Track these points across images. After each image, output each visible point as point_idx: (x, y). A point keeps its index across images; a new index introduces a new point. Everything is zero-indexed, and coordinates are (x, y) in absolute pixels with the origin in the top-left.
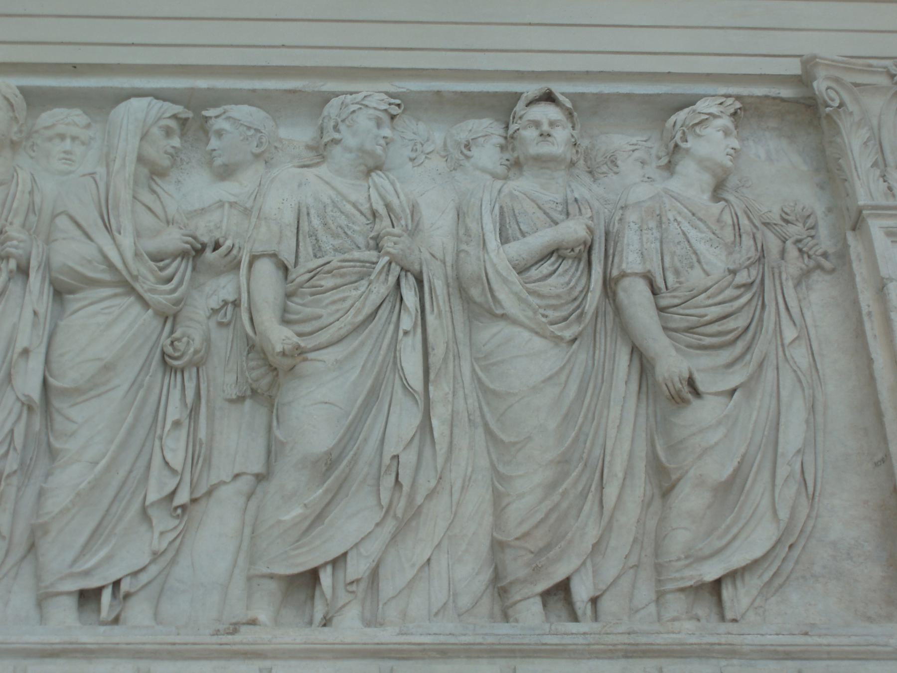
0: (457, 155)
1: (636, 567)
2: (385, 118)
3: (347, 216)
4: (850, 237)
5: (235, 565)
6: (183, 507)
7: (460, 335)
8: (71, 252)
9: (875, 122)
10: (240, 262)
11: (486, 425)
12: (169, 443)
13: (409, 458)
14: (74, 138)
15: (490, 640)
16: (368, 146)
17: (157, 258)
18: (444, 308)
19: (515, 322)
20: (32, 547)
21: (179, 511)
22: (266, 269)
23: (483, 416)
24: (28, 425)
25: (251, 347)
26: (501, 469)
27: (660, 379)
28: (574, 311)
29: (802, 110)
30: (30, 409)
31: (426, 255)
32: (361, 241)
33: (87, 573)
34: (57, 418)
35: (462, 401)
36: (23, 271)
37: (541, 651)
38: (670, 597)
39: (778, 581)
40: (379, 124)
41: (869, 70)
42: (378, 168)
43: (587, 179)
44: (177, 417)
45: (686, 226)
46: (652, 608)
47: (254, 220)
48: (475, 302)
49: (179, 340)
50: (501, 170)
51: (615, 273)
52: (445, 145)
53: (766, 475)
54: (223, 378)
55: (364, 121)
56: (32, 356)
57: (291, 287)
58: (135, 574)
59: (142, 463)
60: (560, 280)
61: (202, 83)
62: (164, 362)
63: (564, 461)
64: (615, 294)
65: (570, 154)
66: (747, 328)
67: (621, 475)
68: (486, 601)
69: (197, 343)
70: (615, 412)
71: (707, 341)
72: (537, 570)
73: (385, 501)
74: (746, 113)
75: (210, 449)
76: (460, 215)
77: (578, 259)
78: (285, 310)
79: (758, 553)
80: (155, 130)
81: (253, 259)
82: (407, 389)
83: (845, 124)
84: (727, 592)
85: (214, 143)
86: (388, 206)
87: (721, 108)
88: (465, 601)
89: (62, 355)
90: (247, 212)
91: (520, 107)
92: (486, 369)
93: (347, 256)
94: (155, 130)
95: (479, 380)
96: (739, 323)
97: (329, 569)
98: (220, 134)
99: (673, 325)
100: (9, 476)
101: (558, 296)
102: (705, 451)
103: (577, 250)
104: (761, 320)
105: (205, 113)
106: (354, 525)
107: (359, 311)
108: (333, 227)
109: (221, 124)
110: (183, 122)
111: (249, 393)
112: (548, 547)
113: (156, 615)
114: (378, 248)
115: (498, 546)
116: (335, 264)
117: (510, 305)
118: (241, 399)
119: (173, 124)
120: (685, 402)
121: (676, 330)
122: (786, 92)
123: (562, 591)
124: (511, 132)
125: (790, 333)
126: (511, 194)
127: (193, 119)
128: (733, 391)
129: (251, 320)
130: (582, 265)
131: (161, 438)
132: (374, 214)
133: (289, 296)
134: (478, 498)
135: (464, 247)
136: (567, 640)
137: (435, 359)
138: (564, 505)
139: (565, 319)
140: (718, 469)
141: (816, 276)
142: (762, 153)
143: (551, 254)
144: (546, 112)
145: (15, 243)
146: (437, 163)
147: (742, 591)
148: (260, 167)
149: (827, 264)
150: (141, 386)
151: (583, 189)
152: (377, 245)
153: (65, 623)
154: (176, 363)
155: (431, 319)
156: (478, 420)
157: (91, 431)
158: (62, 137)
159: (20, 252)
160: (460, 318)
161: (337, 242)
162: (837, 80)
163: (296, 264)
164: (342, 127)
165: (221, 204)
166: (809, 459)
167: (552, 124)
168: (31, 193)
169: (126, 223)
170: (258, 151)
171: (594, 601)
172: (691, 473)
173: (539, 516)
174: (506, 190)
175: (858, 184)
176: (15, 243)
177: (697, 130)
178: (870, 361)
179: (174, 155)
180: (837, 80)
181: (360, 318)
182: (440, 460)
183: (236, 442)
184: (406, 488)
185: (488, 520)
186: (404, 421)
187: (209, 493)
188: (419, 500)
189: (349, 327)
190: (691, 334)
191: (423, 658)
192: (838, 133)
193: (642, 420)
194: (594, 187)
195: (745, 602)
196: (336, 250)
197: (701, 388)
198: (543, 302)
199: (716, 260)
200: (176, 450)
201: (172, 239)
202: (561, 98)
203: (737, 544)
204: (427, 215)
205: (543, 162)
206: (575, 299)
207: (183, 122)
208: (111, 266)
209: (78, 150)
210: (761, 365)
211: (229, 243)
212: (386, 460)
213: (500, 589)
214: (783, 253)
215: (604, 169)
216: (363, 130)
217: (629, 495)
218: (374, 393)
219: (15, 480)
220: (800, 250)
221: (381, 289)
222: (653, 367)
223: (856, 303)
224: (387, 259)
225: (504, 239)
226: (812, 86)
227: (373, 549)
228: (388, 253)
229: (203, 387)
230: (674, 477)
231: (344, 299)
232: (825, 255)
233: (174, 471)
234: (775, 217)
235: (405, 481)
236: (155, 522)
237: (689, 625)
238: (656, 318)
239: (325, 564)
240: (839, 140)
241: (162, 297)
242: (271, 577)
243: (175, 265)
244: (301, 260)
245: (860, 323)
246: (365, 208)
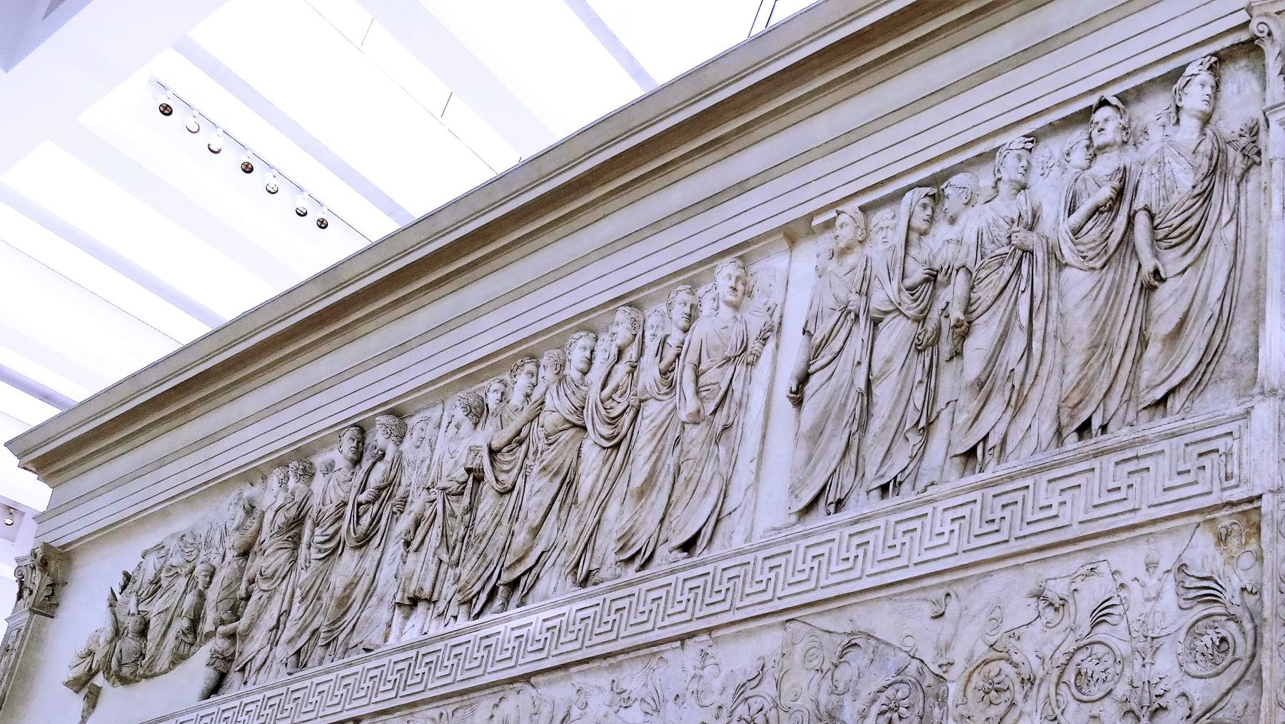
1: (1129, 400)
19: (1072, 266)
33: (882, 476)
36: (857, 316)
42: (1024, 187)
63: (1094, 347)
71: (1174, 241)
79: (1186, 375)
82: (1021, 327)
88: (1044, 445)
112: (1076, 405)
118: (951, 358)
119: (926, 200)
120: (1155, 288)
138: (1090, 374)
144: (1105, 112)
153: (876, 503)
184: (1017, 387)
195: (1178, 406)
205: (1102, 149)
219: (857, 436)
227: (1001, 429)
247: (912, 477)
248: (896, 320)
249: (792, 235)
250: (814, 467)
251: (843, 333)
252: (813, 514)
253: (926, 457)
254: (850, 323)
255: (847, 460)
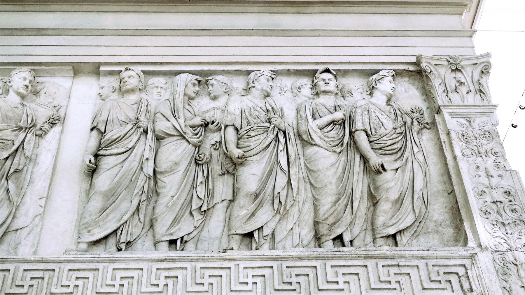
0: (295, 91)
1: (365, 230)
2: (270, 79)
3: (258, 112)
4: (436, 116)
5: (223, 231)
6: (205, 211)
7: (299, 152)
8: (162, 126)
9: (443, 78)
10: (221, 128)
11: (310, 182)
12: (199, 189)
13: (284, 194)
14: (161, 88)
15: (316, 253)
16: (265, 88)
17: (192, 127)
18: (294, 142)
20: (152, 226)
21: (203, 213)
22: (230, 130)
23: (309, 179)
24: (149, 185)
25: (226, 156)
26: (316, 196)
27: (372, 165)
28: (340, 143)
29: (418, 73)
30: (149, 178)
31: (286, 125)
32: (264, 120)
33: (172, 234)
34: (158, 181)
35: (301, 174)
36: (146, 132)
37: (334, 257)
38: (377, 240)
39: (416, 235)
40: (268, 80)
41: (440, 60)
42: (268, 96)
43: (342, 99)
44: (201, 180)
45: (378, 114)
46: (372, 244)
47: (225, 114)
48: (305, 141)
49: (201, 154)
50: (312, 96)
51: (354, 130)
52: (291, 88)
53: (410, 198)
54: (216, 168)
55: (263, 79)
56: (149, 161)
57: (239, 136)
58: (189, 234)
59: (190, 196)
60: (334, 133)
61: (205, 68)
62: (196, 163)
64: (354, 137)
65: (336, 90)
66: (401, 148)
67: (359, 199)
68: (313, 243)
69: (207, 156)
70: (356, 177)
71: (387, 152)
72: (331, 231)
73: (276, 208)
74: (397, 74)
75: (213, 192)
76: (298, 111)
77: (340, 125)
78: (238, 144)
79: (409, 225)
80: (190, 84)
81: (226, 127)
82: (282, 169)
83: (431, 77)
84: (398, 238)
85: (210, 88)
86: (272, 108)
87: (388, 74)
88: (305, 242)
89: (160, 160)
90: (223, 111)
91: (317, 75)
92: (309, 163)
93: (259, 125)
94: (190, 84)
95: (307, 167)
96: (398, 146)
97: (257, 231)
98: (212, 85)
99: (374, 147)
100: (143, 202)
101: (334, 137)
102: (388, 189)
103: (340, 122)
104: (406, 145)
105: (207, 78)
106: (265, 216)
107: (264, 143)
108: (254, 115)
109: (212, 82)
110: (199, 82)
111: (226, 172)
112: (334, 223)
113: (196, 249)
114: (270, 122)
115: (316, 223)
116: (255, 128)
117: (317, 140)
118: (224, 174)
119: (196, 82)
120: (381, 173)
121: (376, 149)
122: (411, 68)
123: (339, 239)
124: (314, 83)
125: (416, 150)
126: (315, 103)
127: (203, 79)
128: (397, 169)
129: (226, 147)
130: (342, 127)
131: (196, 188)
132: (268, 111)
133: (239, 139)
134: (308, 207)
135: (300, 121)
136: (343, 253)
137: (292, 159)
138: (339, 208)
139: (337, 145)
140: (394, 195)
141: (424, 130)
142: (403, 89)
143: (331, 123)
145: (142, 122)
146: (289, 94)
147: (403, 238)
148: (227, 96)
149: (428, 127)
150: (188, 170)
151: (340, 101)
152: (269, 121)
153: (164, 251)
154: (200, 162)
155: (289, 146)
156: (307, 180)
157: (171, 185)
158: (157, 87)
159: (144, 125)
160: (300, 146)
161: (255, 121)
162: (429, 63)
163: (241, 128)
164: (255, 82)
165: (214, 109)
166: (425, 192)
167: (329, 80)
168: (147, 106)
169: (181, 114)
170: (226, 91)
171: (351, 241)
172: (384, 197)
173: (331, 212)
174: (314, 103)
175: (438, 98)
176: (142, 122)
177: (380, 81)
178: (445, 158)
179: (197, 93)
180: (429, 63)
181: (265, 146)
182: (295, 194)
183: (222, 188)
185: (312, 215)
186: (282, 180)
187: (213, 207)
188: (288, 208)
189: (261, 149)
190: (382, 150)
191: (292, 260)
192: (431, 81)
193: (365, 180)
194: (344, 101)
196: (255, 123)
197: (386, 167)
198: (329, 139)
199: (389, 125)
200: (201, 191)
201: (198, 121)
202: (332, 71)
203: (401, 221)
204: (286, 111)
205: (325, 92)
206: (340, 139)
207: (199, 82)
208: (177, 130)
209: (163, 92)
210: (407, 160)
211: (217, 122)
212: (276, 194)
213: (318, 238)
214: (412, 123)
215: (348, 95)
216: (262, 83)
217: (361, 205)
218: (271, 172)
219: (145, 203)
220: (418, 122)
221: (271, 136)
222: (369, 162)
223: (439, 139)
224: (273, 126)
225: (314, 119)
226: (420, 66)
228: (273, 124)
229: (210, 171)
230: (378, 199)
231: (259, 140)
232: (427, 123)
233: (201, 199)
234: (409, 111)
235: (283, 201)
236: (195, 216)
237: (386, 248)
238: (369, 144)
239: (256, 230)
240: (430, 83)
241: (194, 140)
242: (237, 234)
243: (199, 129)
244: (243, 127)
245: (441, 145)
246: (264, 109)
247: (195, 240)
248: (179, 141)
249: (77, 70)
250: (108, 215)
251: (135, 138)
252: (101, 247)
253: (205, 229)
254: (139, 134)
255: (136, 217)
